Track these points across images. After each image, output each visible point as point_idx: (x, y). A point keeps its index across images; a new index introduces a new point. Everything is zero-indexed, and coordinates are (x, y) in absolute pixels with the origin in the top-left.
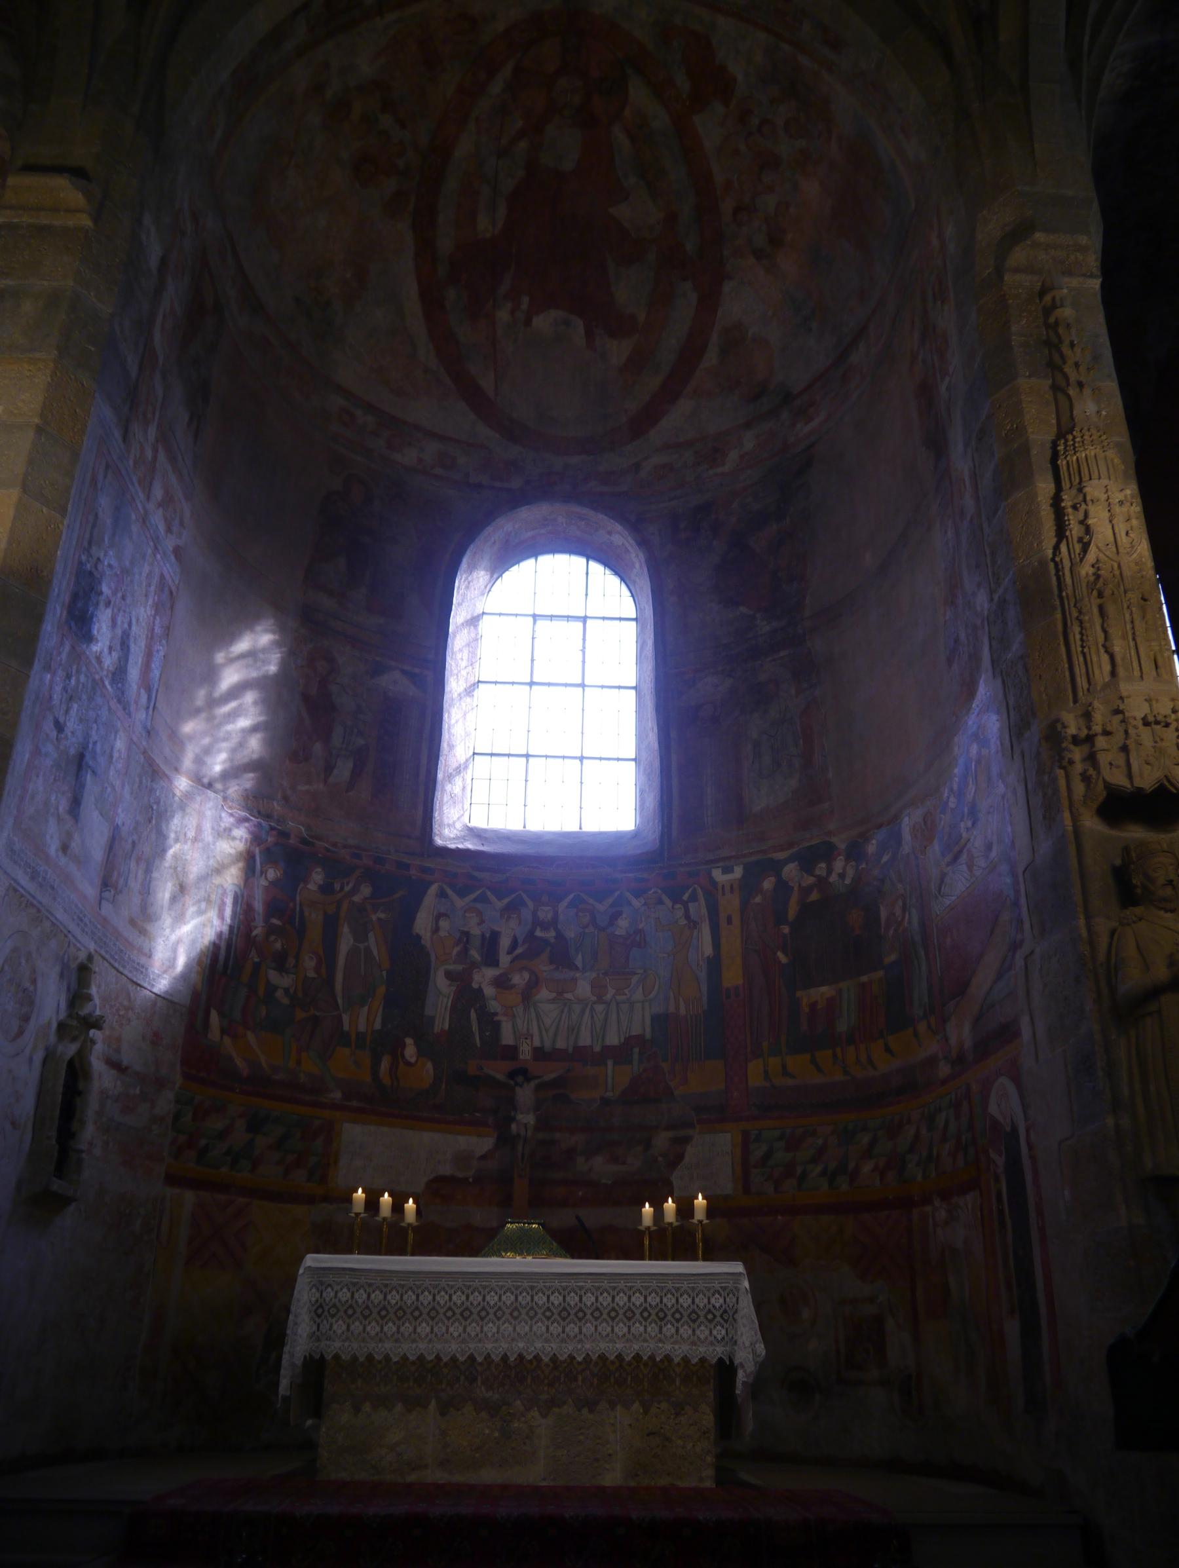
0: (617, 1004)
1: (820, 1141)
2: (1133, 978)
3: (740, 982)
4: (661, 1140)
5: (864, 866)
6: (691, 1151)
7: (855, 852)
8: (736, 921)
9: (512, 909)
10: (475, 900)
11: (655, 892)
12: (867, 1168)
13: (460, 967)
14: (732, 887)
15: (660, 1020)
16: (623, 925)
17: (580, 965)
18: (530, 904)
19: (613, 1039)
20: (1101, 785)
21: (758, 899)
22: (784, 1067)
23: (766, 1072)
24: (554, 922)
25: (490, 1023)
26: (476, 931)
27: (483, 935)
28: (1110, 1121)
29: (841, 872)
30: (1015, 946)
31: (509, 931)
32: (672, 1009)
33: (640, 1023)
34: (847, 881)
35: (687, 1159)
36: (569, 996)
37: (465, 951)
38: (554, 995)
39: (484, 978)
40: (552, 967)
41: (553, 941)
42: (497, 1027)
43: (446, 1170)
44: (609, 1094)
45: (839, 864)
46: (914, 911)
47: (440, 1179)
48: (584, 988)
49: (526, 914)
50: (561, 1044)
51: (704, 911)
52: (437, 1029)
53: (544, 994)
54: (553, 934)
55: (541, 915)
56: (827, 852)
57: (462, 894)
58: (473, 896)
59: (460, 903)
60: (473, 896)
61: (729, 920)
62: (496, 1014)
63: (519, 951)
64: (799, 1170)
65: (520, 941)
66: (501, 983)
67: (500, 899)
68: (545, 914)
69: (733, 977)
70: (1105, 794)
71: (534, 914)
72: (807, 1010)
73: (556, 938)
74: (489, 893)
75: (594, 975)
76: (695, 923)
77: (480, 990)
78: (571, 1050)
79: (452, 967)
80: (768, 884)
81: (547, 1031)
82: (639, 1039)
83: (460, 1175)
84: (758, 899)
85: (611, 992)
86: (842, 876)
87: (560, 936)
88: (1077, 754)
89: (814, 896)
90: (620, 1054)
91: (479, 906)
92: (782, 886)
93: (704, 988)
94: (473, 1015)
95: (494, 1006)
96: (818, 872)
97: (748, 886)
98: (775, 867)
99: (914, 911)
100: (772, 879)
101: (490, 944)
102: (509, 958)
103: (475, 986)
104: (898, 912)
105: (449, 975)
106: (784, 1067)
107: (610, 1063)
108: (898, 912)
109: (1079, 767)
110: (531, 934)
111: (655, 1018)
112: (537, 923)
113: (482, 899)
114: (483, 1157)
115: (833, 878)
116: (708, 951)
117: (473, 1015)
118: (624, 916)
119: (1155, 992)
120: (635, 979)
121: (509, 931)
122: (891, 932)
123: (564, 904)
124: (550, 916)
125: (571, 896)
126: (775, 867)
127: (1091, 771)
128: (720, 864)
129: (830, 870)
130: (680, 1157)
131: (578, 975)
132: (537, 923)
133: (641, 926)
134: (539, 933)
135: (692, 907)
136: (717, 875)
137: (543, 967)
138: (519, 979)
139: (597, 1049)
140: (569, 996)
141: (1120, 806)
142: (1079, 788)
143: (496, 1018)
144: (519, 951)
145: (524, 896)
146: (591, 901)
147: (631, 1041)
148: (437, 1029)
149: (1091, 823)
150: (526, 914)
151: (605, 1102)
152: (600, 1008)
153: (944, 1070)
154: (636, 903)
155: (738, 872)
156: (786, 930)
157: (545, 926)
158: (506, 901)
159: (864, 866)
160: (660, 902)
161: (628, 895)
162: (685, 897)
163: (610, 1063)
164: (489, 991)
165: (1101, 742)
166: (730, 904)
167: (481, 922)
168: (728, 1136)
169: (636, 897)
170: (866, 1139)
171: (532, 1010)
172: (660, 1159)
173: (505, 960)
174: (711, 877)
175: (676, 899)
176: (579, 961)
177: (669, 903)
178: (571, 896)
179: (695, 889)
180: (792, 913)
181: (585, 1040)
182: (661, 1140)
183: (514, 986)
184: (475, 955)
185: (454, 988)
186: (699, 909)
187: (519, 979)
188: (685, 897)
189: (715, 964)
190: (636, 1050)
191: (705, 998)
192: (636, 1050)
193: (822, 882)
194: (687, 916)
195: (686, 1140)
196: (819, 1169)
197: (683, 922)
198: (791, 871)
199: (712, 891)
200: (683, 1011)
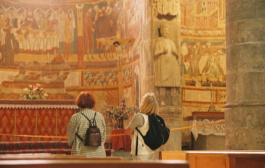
0: (50, 39)
1: (100, 75)
2: (157, 52)
3: (82, 35)
4: (62, 73)
5: (114, 9)
6: (69, 76)
7: (112, 5)
8: (82, 19)
9: (21, 12)
10: (10, 9)
11: (60, 10)
12: (110, 81)
13: (7, 28)
14: (81, 10)
15: (61, 43)
16: (51, 18)
17: (40, 28)
18: (26, 11)
19: (49, 48)
20: (157, 13)
21: (87, 14)
22: (92, 57)
23: (88, 58)
24: (32, 16)
25: (16, 43)
26: (11, 18)
27: (13, 19)
28: (151, 76)
29: (109, 10)
30: (141, 40)
31: (20, 18)
32: (64, 41)
33: (56, 44)
34: (110, 13)
35: (68, 78)
36: (37, 36)
37: (8, 23)
38: (33, 36)
39: (14, 31)
40: (33, 28)
41: (32, 21)
42: (18, 44)
43: (6, 80)
44: (48, 62)
45: (108, 8)
46: (124, 24)
47: (4, 82)
48: (41, 34)
49: (25, 13)
50: (35, 49)
51: (73, 16)
52: (2, 44)
53: (30, 35)
54: (32, 19)
55: (29, 14)
56: (105, 4)
57: (6, 7)
58: (10, 8)
59: (6, 10)
60: (10, 8)
61: (80, 19)
62: (17, 41)
63: (23, 24)
64: (95, 81)
65: (23, 21)
66: (19, 32)
67: (17, 9)
68: (30, 14)
69: (80, 34)
70: (158, 14)
71: (27, 13)
72: (98, 43)
73: (33, 20)
74: (14, 8)
75: (44, 31)
76: (71, 19)
77: (13, 34)
78: (38, 50)
79: (5, 28)
80: (90, 10)
81: (31, 46)
82: (56, 48)
83: (10, 81)
84: (87, 14)
85: (48, 36)
86: (109, 11)
87: (34, 20)
88: (154, 5)
89: (102, 15)
90: (51, 52)
91: (12, 11)
92: (93, 11)
93: (73, 36)
94: (11, 41)
95: (17, 38)
96: (103, 9)
97: (85, 10)
98: (92, 6)
99: (124, 24)
100: (91, 9)
101: (15, 21)
102: (21, 25)
103: (11, 33)
104: (121, 23)
105: (4, 30)
106: (92, 57)
107: (48, 54)
108: (121, 23)
109: (154, 7)
110: (26, 19)
111: (60, 43)
112: (27, 16)
113: (12, 9)
114: (16, 77)
115: (106, 11)
116: (74, 26)
117: (11, 41)
118: (51, 16)
119: (161, 54)
120: (55, 33)
121: (20, 18)
122: (119, 28)
123: (35, 11)
124: (31, 14)
125: (37, 9)
126: (92, 6)
127: (156, 9)
128: (78, 4)
129: (106, 9)
130: (66, 77)
131: (39, 31)
132: (27, 16)
133: (56, 18)
134: (28, 19)
135: (70, 14)
136: (77, 6)
137: (30, 28)
138: (23, 31)
139: (45, 50)
140: (37, 36)
141: (160, 17)
142: (153, 12)
143: (18, 42)
144: (23, 24)
145: (24, 9)
146: (43, 11)
147: (53, 49)
148: (2, 44)
149: (156, 19)
150: (25, 13)
151: (47, 64)
152: (45, 40)
153: (128, 61)
154: (54, 12)
155: (83, 6)
156: (94, 23)
157: (30, 17)
158: (19, 10)
159: (114, 9)
160: (62, 12)
161: (52, 10)
162: (68, 12)
163: (48, 54)
164: (15, 34)
165: (158, 3)
166: (80, 15)
167: (12, 15)
168: (78, 72)
169: (55, 10)
170: (111, 75)
171: (27, 39)
172: (61, 78)
173: (19, 26)
174: (75, 7)
175: (66, 12)
176: (40, 27)
177: (64, 13)
178: (37, 9)
179: (71, 10)
180: (96, 19)
181: (42, 48)
182: (62, 73)
183: (22, 33)
184: (11, 24)
185: (6, 34)
186: (72, 15)
187: (23, 31)
188: (68, 12)
189: (76, 30)
190: (55, 51)
191: (73, 39)
192: (55, 51)
193: (104, 12)
194: (69, 17)
195: (68, 73)
196: (100, 80)
197: (67, 18)
198: (96, 7)
199: (75, 10)
200: (67, 42)
